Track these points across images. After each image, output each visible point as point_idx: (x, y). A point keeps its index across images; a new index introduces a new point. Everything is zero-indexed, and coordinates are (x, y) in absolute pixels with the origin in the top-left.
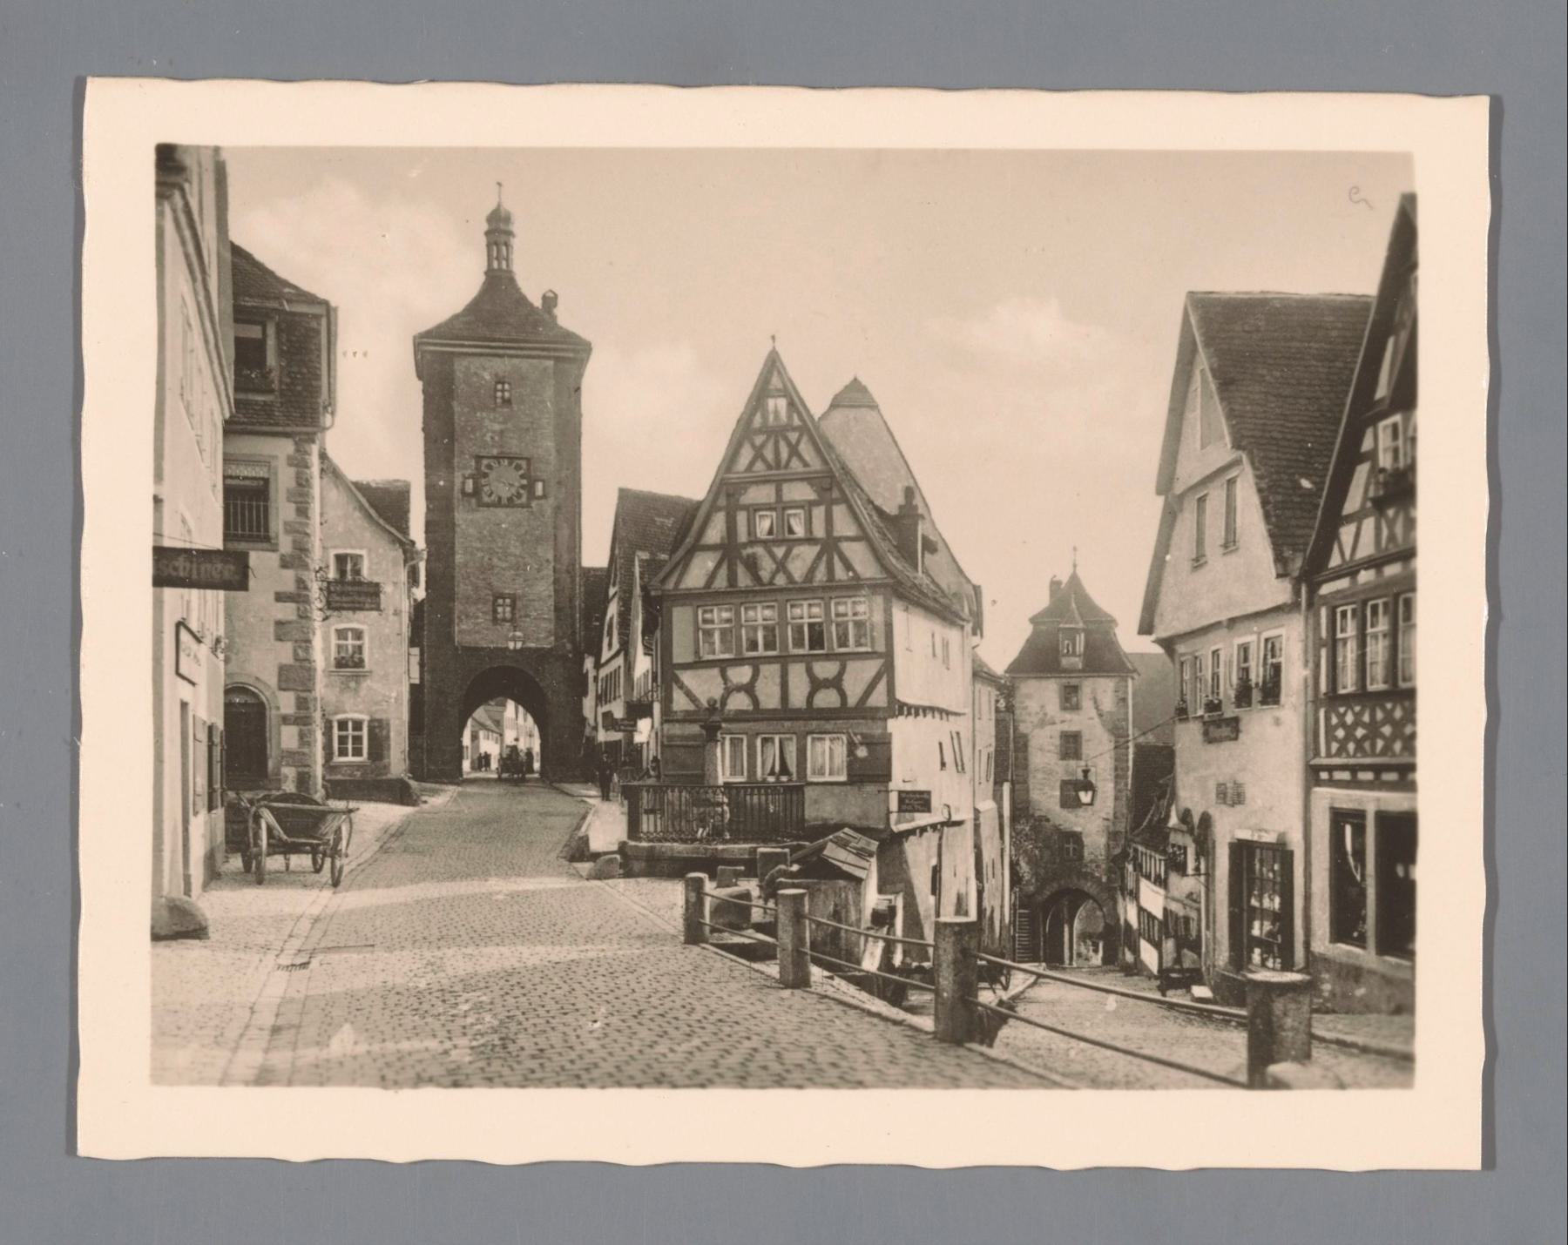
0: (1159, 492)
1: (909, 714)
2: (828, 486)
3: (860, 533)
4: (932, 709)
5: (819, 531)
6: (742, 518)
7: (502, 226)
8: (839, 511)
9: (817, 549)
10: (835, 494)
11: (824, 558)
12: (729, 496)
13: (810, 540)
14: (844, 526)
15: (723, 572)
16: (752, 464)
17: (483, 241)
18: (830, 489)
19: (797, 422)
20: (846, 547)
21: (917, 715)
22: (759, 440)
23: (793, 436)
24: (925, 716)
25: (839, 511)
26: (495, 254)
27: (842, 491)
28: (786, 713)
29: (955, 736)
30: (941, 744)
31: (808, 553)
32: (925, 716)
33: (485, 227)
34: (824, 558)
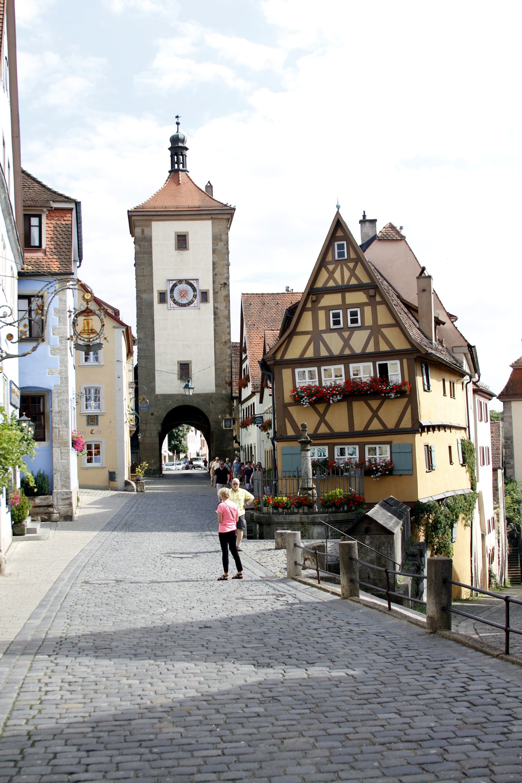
1: (428, 430)
2: (374, 294)
4: (444, 427)
5: (369, 322)
6: (322, 314)
7: (180, 145)
8: (381, 309)
9: (368, 332)
10: (378, 299)
12: (313, 302)
13: (362, 328)
14: (383, 317)
15: (311, 347)
16: (327, 281)
17: (169, 153)
18: (375, 296)
19: (353, 256)
20: (384, 330)
21: (434, 430)
22: (331, 267)
23: (351, 265)
24: (439, 431)
27: (382, 296)
28: (352, 434)
29: (460, 442)
30: (450, 447)
31: (364, 335)
32: (439, 431)
33: (169, 145)
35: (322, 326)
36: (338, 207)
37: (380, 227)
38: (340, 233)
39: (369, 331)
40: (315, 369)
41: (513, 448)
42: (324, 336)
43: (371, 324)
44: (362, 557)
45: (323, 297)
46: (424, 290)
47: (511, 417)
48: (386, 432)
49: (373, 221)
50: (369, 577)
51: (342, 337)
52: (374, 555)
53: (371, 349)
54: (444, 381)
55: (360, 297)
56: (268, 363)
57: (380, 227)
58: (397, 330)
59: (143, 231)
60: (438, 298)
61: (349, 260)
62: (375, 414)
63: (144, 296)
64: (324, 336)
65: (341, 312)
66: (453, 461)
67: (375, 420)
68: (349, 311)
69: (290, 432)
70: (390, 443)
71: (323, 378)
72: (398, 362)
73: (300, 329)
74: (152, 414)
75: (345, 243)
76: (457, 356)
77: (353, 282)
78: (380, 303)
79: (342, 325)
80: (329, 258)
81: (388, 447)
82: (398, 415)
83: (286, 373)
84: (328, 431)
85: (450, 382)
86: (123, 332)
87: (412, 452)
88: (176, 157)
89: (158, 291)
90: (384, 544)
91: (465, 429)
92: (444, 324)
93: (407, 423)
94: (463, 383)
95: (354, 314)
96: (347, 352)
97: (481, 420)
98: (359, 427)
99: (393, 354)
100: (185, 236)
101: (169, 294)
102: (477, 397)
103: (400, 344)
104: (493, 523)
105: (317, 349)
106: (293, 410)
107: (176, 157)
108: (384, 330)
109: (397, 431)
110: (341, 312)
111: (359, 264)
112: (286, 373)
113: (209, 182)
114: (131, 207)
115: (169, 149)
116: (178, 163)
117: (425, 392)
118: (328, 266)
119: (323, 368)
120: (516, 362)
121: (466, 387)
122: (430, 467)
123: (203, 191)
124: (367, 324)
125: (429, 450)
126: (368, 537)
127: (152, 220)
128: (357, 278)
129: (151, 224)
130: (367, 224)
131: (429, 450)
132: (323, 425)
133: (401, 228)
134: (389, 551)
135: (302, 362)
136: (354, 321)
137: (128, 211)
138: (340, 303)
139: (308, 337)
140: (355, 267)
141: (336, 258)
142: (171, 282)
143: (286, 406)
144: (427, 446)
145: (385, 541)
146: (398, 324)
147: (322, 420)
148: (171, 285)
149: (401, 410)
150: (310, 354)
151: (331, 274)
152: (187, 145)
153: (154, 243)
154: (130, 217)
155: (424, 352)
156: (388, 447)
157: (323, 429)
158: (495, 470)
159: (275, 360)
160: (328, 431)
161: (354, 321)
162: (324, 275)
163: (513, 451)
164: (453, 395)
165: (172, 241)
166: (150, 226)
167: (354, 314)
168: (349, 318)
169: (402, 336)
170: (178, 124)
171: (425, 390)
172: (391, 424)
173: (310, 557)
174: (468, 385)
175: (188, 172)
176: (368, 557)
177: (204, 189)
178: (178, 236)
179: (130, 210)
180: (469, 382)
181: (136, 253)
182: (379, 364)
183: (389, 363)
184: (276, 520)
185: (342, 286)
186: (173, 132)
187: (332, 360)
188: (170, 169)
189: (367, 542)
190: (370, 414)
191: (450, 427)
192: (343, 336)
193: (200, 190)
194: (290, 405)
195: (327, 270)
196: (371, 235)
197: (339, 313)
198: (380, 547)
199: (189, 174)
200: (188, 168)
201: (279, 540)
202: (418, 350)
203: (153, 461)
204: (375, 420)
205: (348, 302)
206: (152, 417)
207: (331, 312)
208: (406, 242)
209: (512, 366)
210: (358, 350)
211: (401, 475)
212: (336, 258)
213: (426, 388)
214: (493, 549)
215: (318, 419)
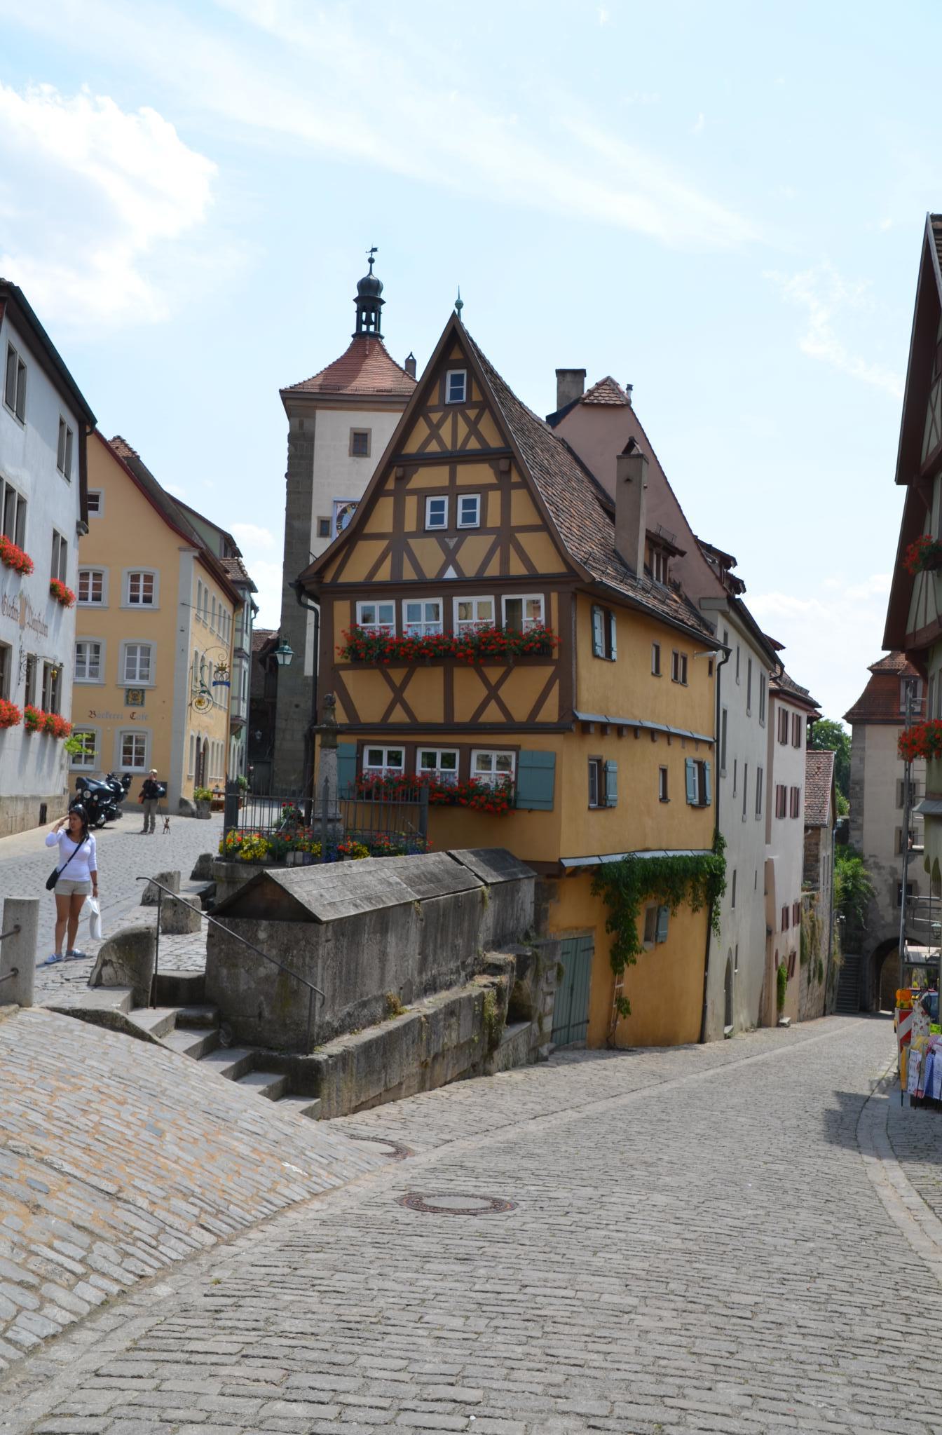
0: (899, 481)
3: (538, 522)
4: (653, 733)
5: (494, 520)
6: (411, 503)
8: (518, 497)
9: (491, 539)
10: (515, 478)
11: (498, 553)
12: (399, 479)
14: (522, 513)
15: (388, 563)
16: (426, 442)
17: (354, 306)
18: (508, 472)
19: (476, 396)
20: (522, 538)
22: (435, 417)
23: (472, 414)
24: (636, 737)
25: (518, 497)
26: (364, 318)
28: (449, 727)
29: (690, 763)
30: (664, 772)
33: (356, 294)
34: (498, 553)
35: (410, 525)
36: (459, 305)
37: (589, 383)
38: (456, 355)
39: (494, 537)
40: (392, 603)
41: (863, 798)
42: (412, 542)
43: (498, 524)
44: (250, 969)
45: (416, 471)
46: (628, 480)
47: (863, 749)
48: (510, 727)
49: (581, 373)
50: (260, 1015)
51: (444, 547)
52: (274, 968)
53: (493, 570)
54: (657, 648)
55: (483, 474)
56: (308, 588)
57: (589, 383)
58: (543, 536)
59: (301, 424)
60: (681, 511)
61: (470, 404)
62: (493, 693)
63: (296, 524)
64: (412, 542)
65: (446, 499)
66: (670, 796)
67: (493, 704)
68: (461, 498)
69: (340, 717)
70: (516, 748)
71: (405, 622)
72: (541, 597)
73: (371, 528)
74: (297, 706)
75: (464, 372)
76: (705, 615)
77: (473, 444)
78: (517, 486)
79: (445, 525)
80: (434, 400)
81: (513, 755)
82: (536, 697)
83: (341, 607)
84: (407, 720)
85: (676, 655)
86: (195, 558)
87: (554, 768)
88: (364, 314)
89: (319, 518)
90: (297, 942)
91: (710, 744)
92: (682, 554)
93: (550, 713)
94: (711, 664)
95: (469, 504)
96: (451, 574)
97: (784, 742)
98: (463, 714)
99: (533, 581)
100: (366, 435)
101: (334, 524)
102: (778, 703)
103: (547, 563)
104: (797, 913)
105: (397, 568)
106: (348, 677)
107: (364, 314)
108: (520, 536)
109: (532, 727)
110: (446, 499)
111: (487, 411)
112: (341, 607)
113: (411, 355)
114: (287, 383)
115: (355, 300)
116: (368, 322)
117: (597, 662)
118: (430, 415)
119: (406, 603)
120: (878, 664)
121: (719, 670)
122: (600, 799)
123: (401, 369)
124: (490, 525)
125: (599, 770)
126: (264, 923)
127: (316, 408)
128: (480, 438)
129: (315, 413)
130: (569, 377)
131: (599, 770)
132: (398, 706)
133: (630, 388)
134: (307, 959)
135: (370, 589)
136: (469, 518)
137: (281, 392)
138: (446, 483)
139: (384, 543)
140: (479, 417)
141: (448, 400)
142: (339, 505)
143: (336, 668)
144: (599, 761)
145: (301, 936)
146: (545, 526)
147: (398, 699)
148: (339, 510)
149: (540, 688)
150: (384, 574)
151: (435, 429)
152: (383, 296)
153: (317, 443)
154: (284, 400)
155: (587, 580)
156: (513, 755)
157: (398, 716)
158: (812, 830)
159: (321, 582)
160: (407, 720)
161: (469, 518)
162: (421, 430)
163: (863, 802)
164: (680, 678)
165: (345, 442)
166: (313, 417)
167: (469, 504)
168: (460, 511)
169: (552, 549)
170: (371, 261)
171: (596, 656)
172: (520, 715)
173: (114, 959)
174: (722, 667)
175: (382, 338)
176: (262, 969)
177: (403, 365)
178: (355, 434)
179: (283, 388)
180: (726, 661)
181: (289, 458)
182: (507, 601)
183: (526, 598)
184: (245, 875)
185: (451, 452)
186: (365, 274)
187: (423, 587)
188: (354, 331)
189: (262, 935)
190: (484, 692)
191: (669, 736)
192: (447, 545)
193: (397, 366)
194: (345, 667)
195: (428, 421)
196: (574, 396)
197: (443, 502)
198: (286, 951)
199: (384, 342)
200: (382, 333)
201: (169, 913)
202: (578, 575)
203: (293, 778)
204: (493, 705)
205: (461, 481)
206: (297, 710)
207: (429, 500)
208: (631, 409)
209: (870, 669)
210: (470, 572)
211: (530, 810)
212: (448, 400)
213: (600, 651)
214: (794, 954)
215: (390, 695)
